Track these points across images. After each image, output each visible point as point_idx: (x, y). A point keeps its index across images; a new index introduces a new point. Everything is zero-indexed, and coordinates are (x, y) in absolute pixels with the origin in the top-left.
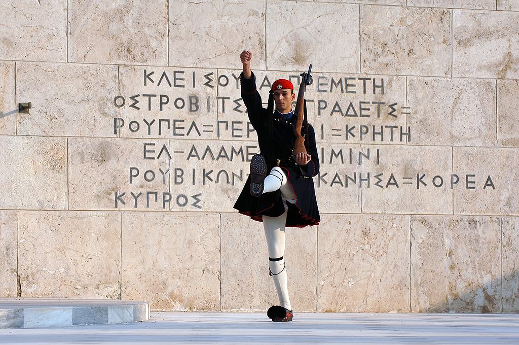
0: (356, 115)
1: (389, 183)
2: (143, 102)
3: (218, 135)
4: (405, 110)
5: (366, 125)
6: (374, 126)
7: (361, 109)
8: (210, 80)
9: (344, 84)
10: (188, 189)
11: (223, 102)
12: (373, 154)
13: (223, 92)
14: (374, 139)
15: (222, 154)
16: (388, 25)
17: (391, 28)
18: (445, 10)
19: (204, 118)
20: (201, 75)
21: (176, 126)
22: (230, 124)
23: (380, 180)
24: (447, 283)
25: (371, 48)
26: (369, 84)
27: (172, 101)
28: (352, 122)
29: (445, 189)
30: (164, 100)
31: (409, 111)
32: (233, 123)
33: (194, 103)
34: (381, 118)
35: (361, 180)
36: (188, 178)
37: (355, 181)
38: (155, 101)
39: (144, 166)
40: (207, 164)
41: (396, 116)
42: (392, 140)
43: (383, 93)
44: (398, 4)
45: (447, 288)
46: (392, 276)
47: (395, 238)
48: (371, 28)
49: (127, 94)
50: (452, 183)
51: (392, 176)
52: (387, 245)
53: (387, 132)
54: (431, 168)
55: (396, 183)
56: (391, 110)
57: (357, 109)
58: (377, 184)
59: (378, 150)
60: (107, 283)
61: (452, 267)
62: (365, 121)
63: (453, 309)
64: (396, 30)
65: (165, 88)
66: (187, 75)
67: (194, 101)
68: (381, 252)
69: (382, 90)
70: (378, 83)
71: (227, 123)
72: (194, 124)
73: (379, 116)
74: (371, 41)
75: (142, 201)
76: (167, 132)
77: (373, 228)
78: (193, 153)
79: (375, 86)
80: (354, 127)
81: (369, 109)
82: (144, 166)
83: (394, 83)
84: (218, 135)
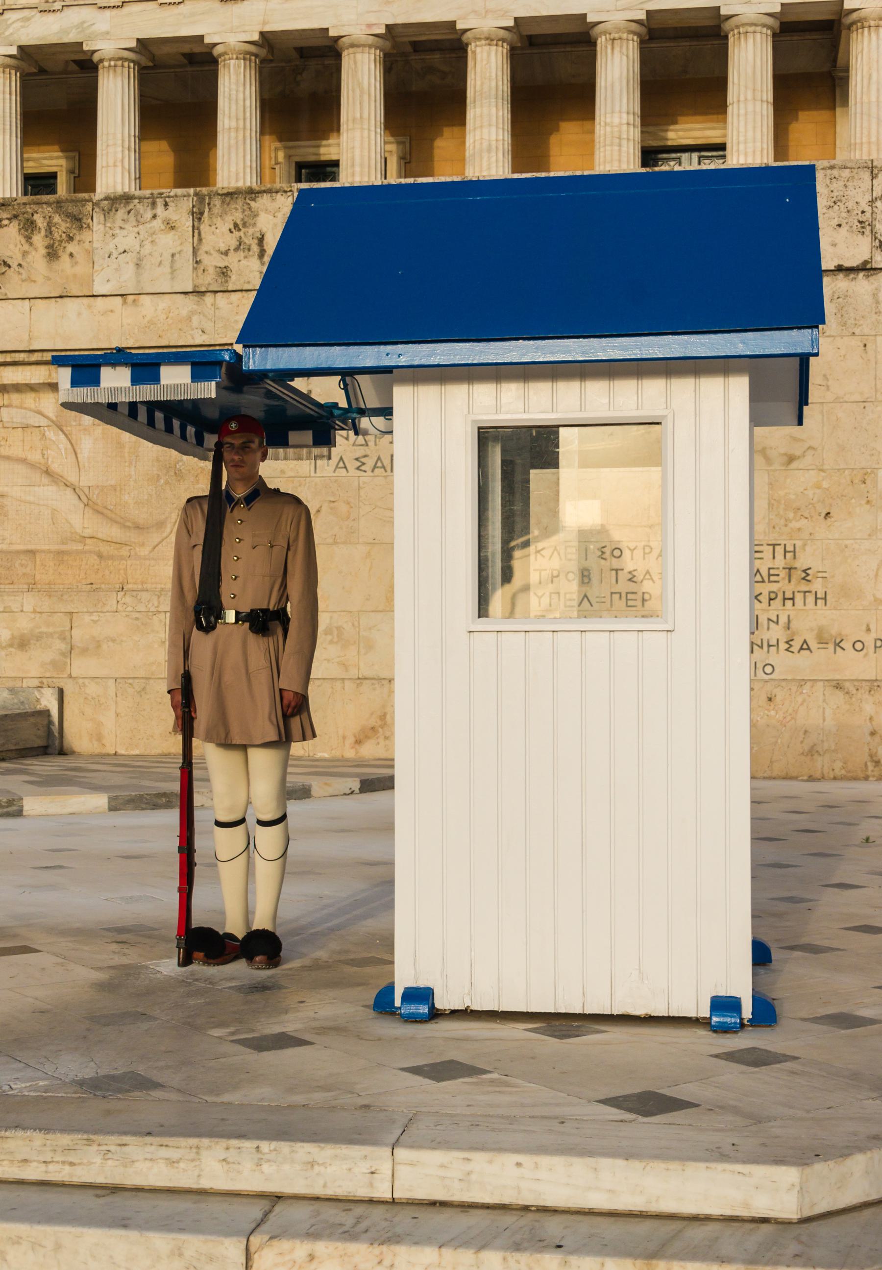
0: (763, 581)
1: (801, 648)
3: (611, 605)
4: (820, 575)
5: (775, 590)
6: (784, 592)
7: (769, 575)
8: (603, 553)
11: (617, 574)
12: (783, 620)
13: (615, 563)
14: (784, 605)
16: (802, 490)
17: (805, 492)
18: (869, 471)
22: (624, 595)
23: (791, 646)
24: (866, 749)
25: (781, 513)
26: (779, 550)
29: (866, 655)
31: (824, 575)
32: (627, 593)
34: (792, 583)
35: (769, 646)
37: (762, 647)
41: (809, 581)
42: (805, 605)
43: (795, 558)
44: (814, 467)
45: (867, 755)
46: (802, 742)
47: (805, 704)
48: (782, 493)
50: (876, 647)
51: (805, 641)
52: (796, 712)
53: (799, 598)
54: (853, 632)
55: (809, 649)
56: (804, 575)
57: (765, 573)
58: (787, 650)
59: (789, 616)
61: (873, 734)
62: (774, 587)
63: (874, 776)
64: (810, 493)
67: (586, 573)
68: (788, 718)
69: (795, 555)
70: (790, 548)
71: (620, 593)
72: (586, 596)
73: (790, 581)
74: (782, 506)
77: (780, 695)
79: (785, 552)
80: (761, 594)
81: (778, 575)
83: (807, 548)
84: (611, 605)
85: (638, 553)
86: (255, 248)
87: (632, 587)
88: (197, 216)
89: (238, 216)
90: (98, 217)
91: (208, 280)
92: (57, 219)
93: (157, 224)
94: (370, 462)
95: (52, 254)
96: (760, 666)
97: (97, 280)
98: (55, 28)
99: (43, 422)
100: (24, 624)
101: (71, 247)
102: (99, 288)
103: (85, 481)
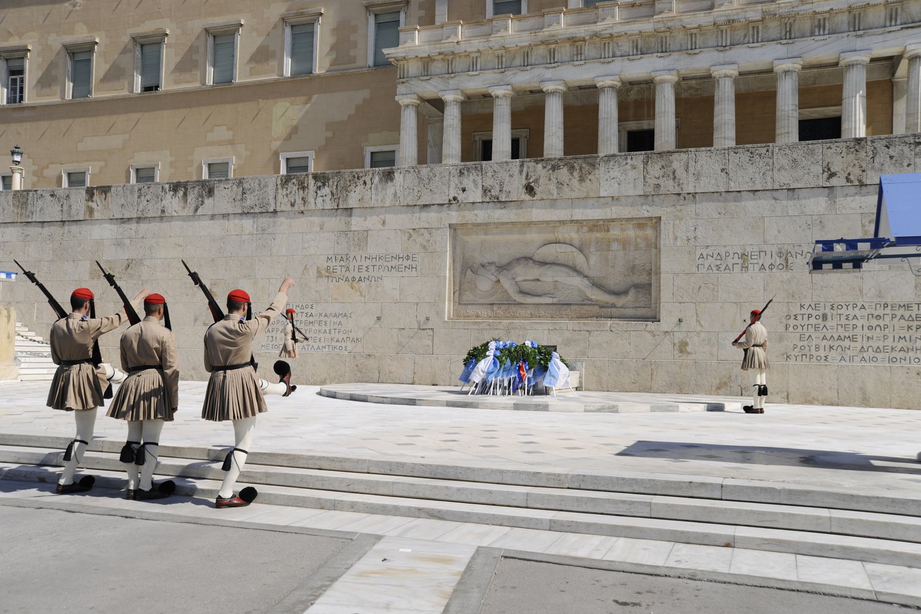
2: (799, 317)
9: (907, 307)
10: (822, 353)
15: (839, 338)
19: (829, 323)
20: (828, 305)
21: (816, 328)
27: (814, 316)
28: (911, 323)
30: (810, 316)
33: (825, 317)
36: (822, 349)
38: (806, 317)
39: (800, 344)
40: (831, 343)
49: (792, 314)
57: (914, 317)
60: (782, 392)
65: (810, 310)
66: (822, 305)
75: (799, 358)
76: (811, 330)
78: (824, 338)
82: (800, 344)
85: (850, 307)
86: (672, 176)
87: (847, 322)
88: (646, 163)
89: (663, 163)
90: (602, 164)
91: (650, 190)
92: (584, 165)
93: (628, 167)
94: (723, 267)
95: (582, 180)
96: (912, 359)
97: (601, 190)
98: (528, 77)
99: (574, 249)
100: (567, 335)
101: (590, 177)
102: (602, 194)
103: (592, 274)
